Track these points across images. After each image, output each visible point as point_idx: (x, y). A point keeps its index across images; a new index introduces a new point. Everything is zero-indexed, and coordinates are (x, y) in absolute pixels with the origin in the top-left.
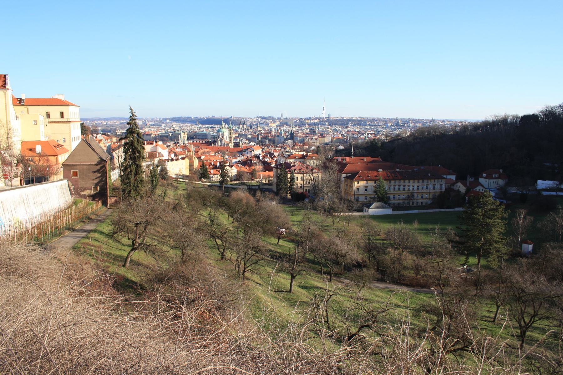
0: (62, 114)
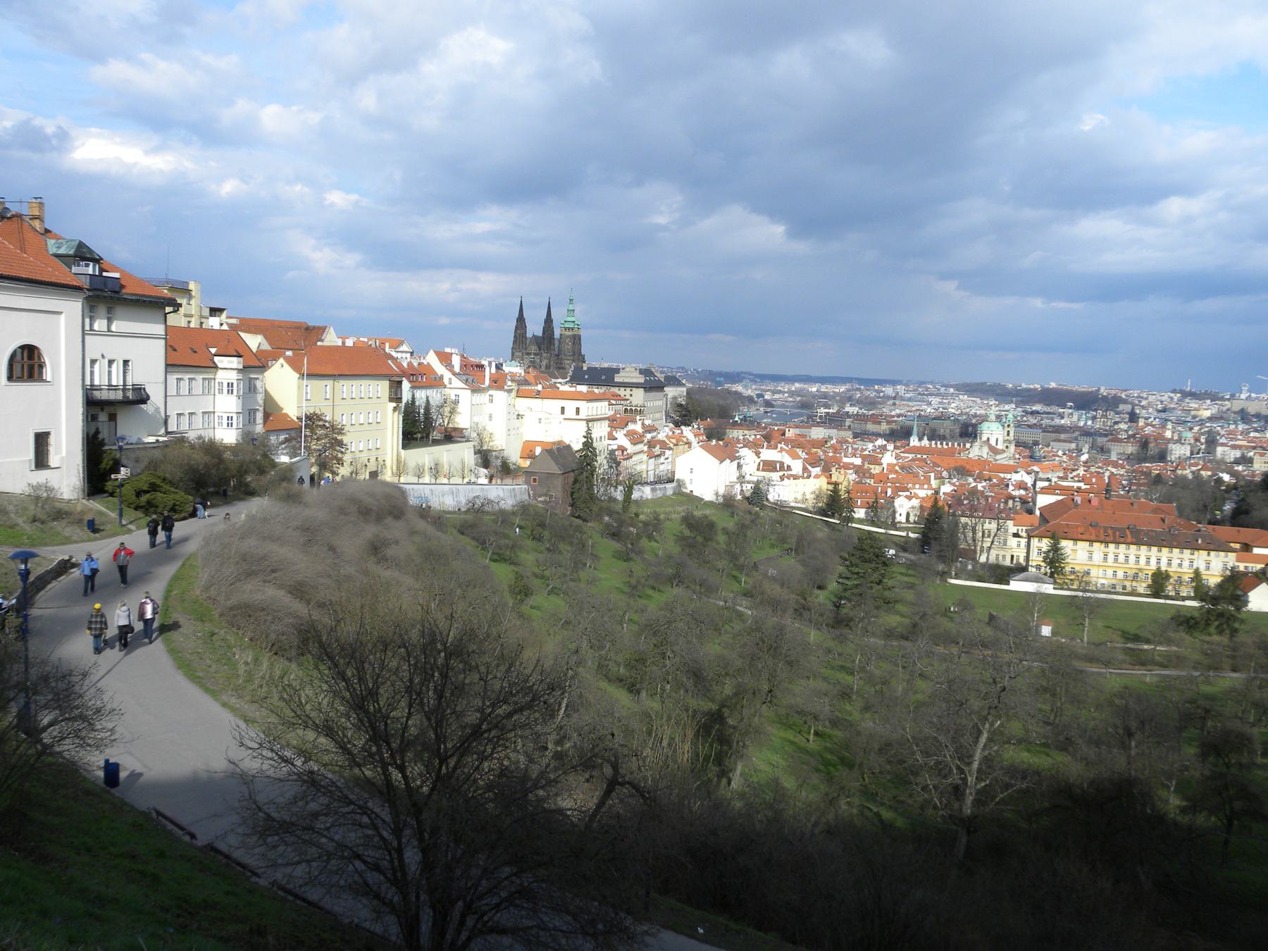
0: (578, 410)
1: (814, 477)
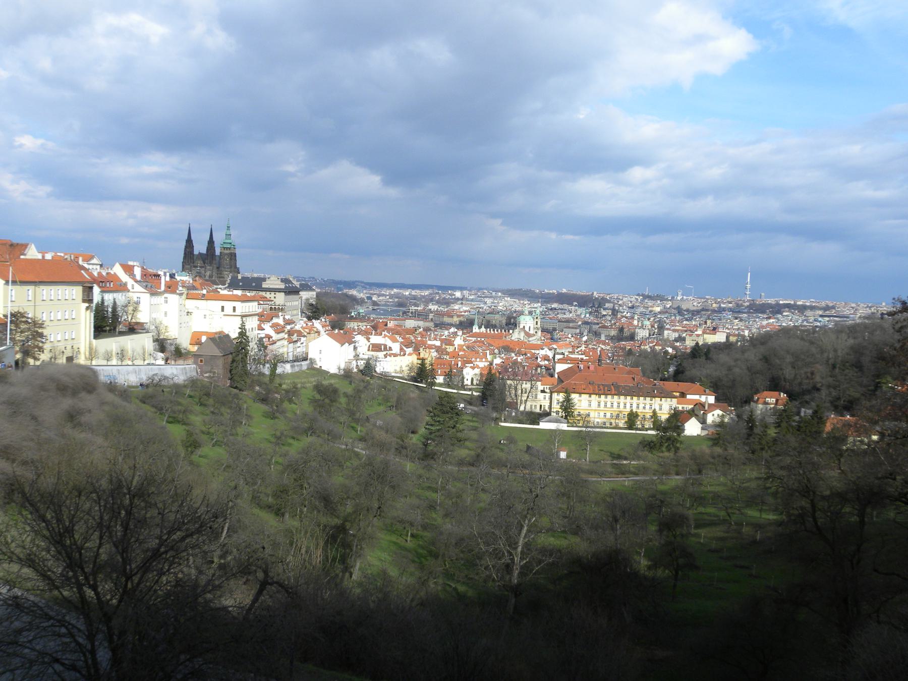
0: (234, 309)
1: (408, 355)
